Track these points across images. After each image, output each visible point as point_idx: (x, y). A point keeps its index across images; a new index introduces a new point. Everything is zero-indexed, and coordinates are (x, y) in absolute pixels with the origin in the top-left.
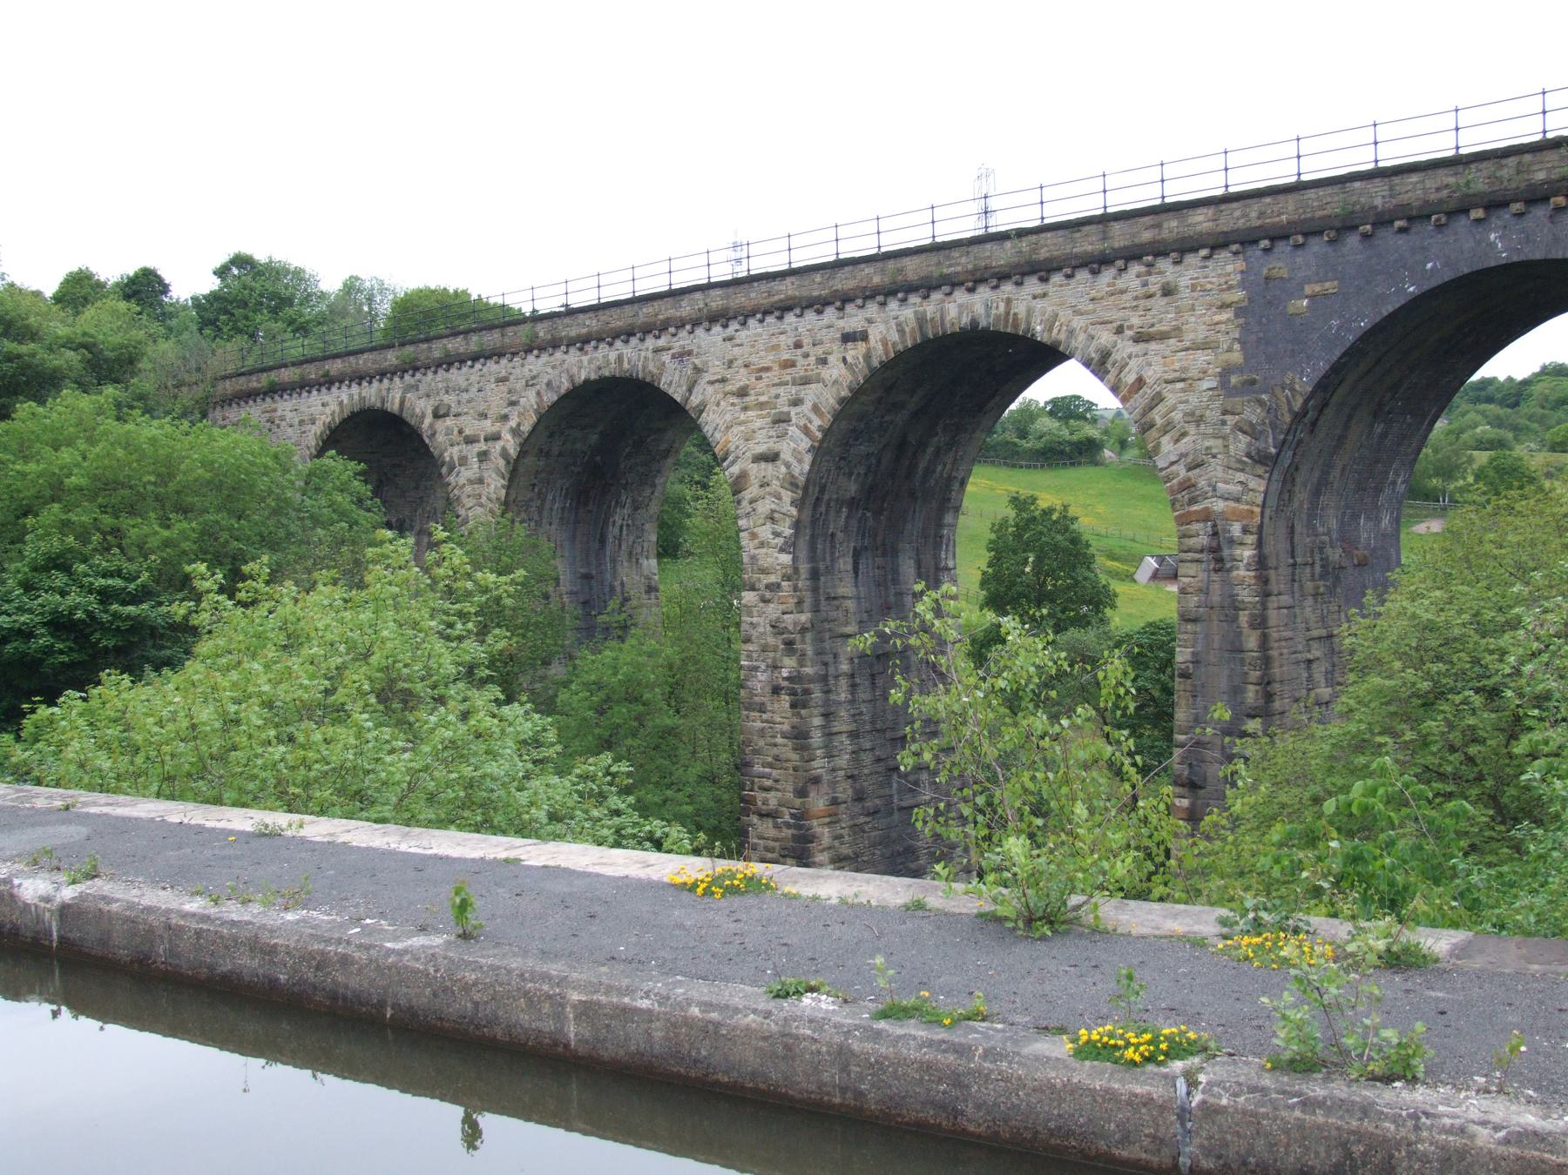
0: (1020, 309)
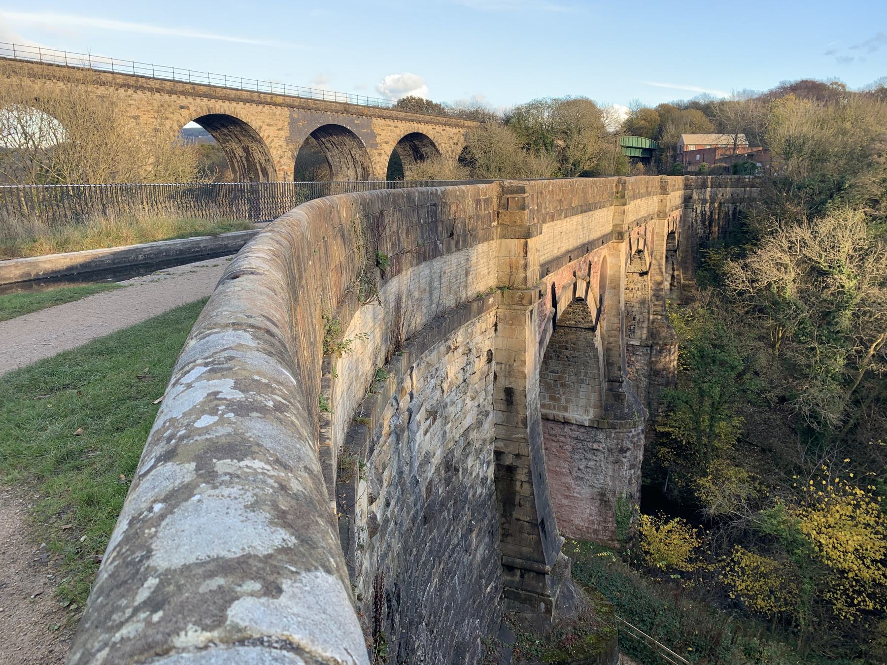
0: (237, 110)
